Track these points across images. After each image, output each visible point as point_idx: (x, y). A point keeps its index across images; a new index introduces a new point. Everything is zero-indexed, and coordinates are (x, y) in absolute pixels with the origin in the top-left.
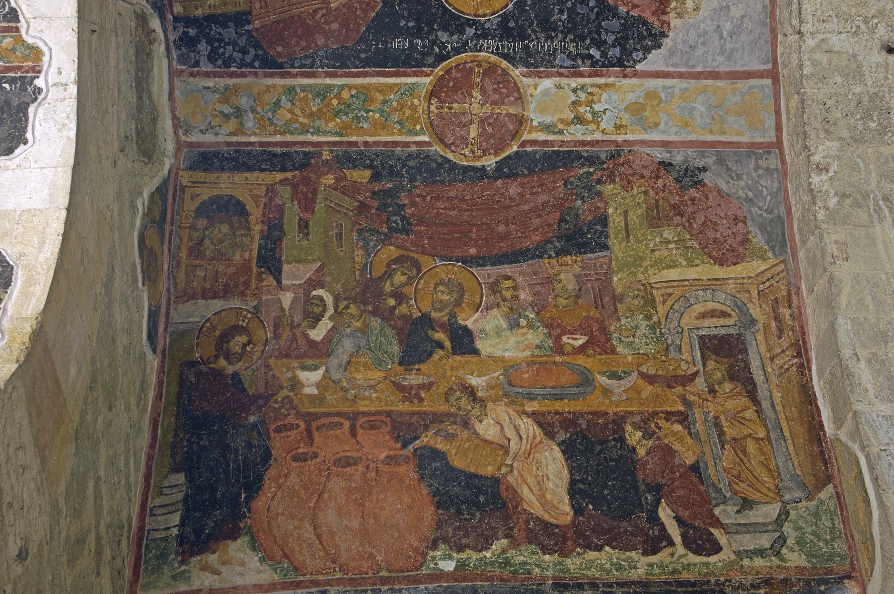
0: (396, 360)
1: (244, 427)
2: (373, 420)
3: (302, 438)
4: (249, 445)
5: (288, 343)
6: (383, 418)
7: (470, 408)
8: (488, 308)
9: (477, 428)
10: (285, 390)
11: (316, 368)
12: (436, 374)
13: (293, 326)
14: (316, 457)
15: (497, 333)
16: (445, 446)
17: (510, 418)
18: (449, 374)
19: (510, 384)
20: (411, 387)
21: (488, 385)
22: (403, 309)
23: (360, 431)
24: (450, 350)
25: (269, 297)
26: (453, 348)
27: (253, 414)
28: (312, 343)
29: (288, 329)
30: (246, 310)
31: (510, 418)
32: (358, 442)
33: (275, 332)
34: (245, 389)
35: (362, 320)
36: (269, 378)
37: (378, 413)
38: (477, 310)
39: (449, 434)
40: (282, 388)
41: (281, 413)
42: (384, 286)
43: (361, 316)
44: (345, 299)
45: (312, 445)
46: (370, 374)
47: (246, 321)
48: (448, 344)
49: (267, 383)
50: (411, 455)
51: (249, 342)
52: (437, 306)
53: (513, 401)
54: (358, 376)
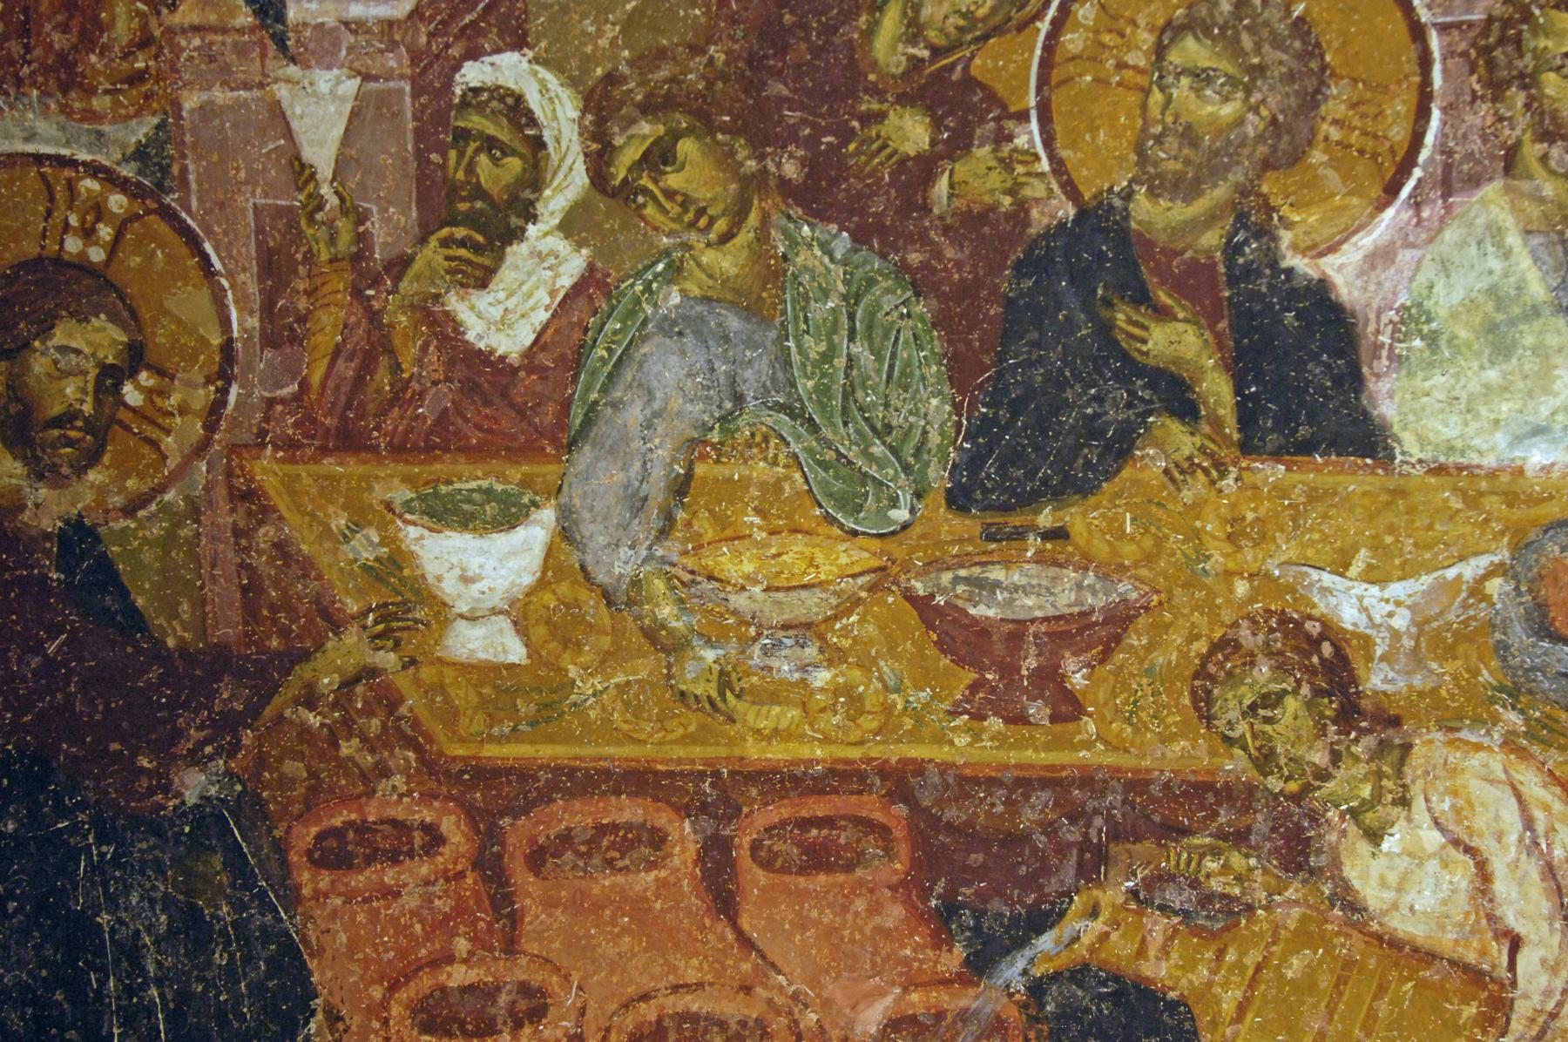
0: (938, 477)
1: (157, 831)
2: (823, 818)
3: (460, 909)
4: (192, 928)
5: (346, 369)
6: (870, 806)
7: (1319, 757)
8: (1452, 180)
9: (1351, 872)
10: (351, 637)
11: (509, 516)
12: (1149, 559)
13: (369, 273)
14: (537, 1014)
15: (1491, 328)
16: (1189, 965)
17: (1529, 823)
18: (1218, 559)
19: (1543, 628)
20: (1017, 631)
21: (1420, 624)
22: (975, 177)
23: (754, 879)
24: (1231, 429)
25: (220, 96)
26: (1247, 416)
27: (195, 759)
28: (478, 371)
29: (338, 285)
30: (94, 170)
31: (1529, 823)
32: (746, 942)
33: (268, 307)
34: (136, 620)
35: (745, 237)
36: (260, 562)
37: (843, 777)
38: (1392, 190)
39: (1207, 899)
40: (336, 623)
41: (343, 764)
42: (869, 33)
43: (739, 214)
44: (647, 109)
45: (511, 947)
46: (795, 551)
47: (105, 232)
48: (1217, 389)
49: (252, 590)
50: (1012, 1014)
51: (135, 357)
52: (1168, 158)
53: (1548, 723)
54: (736, 564)
